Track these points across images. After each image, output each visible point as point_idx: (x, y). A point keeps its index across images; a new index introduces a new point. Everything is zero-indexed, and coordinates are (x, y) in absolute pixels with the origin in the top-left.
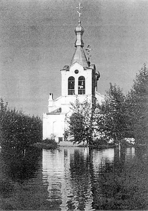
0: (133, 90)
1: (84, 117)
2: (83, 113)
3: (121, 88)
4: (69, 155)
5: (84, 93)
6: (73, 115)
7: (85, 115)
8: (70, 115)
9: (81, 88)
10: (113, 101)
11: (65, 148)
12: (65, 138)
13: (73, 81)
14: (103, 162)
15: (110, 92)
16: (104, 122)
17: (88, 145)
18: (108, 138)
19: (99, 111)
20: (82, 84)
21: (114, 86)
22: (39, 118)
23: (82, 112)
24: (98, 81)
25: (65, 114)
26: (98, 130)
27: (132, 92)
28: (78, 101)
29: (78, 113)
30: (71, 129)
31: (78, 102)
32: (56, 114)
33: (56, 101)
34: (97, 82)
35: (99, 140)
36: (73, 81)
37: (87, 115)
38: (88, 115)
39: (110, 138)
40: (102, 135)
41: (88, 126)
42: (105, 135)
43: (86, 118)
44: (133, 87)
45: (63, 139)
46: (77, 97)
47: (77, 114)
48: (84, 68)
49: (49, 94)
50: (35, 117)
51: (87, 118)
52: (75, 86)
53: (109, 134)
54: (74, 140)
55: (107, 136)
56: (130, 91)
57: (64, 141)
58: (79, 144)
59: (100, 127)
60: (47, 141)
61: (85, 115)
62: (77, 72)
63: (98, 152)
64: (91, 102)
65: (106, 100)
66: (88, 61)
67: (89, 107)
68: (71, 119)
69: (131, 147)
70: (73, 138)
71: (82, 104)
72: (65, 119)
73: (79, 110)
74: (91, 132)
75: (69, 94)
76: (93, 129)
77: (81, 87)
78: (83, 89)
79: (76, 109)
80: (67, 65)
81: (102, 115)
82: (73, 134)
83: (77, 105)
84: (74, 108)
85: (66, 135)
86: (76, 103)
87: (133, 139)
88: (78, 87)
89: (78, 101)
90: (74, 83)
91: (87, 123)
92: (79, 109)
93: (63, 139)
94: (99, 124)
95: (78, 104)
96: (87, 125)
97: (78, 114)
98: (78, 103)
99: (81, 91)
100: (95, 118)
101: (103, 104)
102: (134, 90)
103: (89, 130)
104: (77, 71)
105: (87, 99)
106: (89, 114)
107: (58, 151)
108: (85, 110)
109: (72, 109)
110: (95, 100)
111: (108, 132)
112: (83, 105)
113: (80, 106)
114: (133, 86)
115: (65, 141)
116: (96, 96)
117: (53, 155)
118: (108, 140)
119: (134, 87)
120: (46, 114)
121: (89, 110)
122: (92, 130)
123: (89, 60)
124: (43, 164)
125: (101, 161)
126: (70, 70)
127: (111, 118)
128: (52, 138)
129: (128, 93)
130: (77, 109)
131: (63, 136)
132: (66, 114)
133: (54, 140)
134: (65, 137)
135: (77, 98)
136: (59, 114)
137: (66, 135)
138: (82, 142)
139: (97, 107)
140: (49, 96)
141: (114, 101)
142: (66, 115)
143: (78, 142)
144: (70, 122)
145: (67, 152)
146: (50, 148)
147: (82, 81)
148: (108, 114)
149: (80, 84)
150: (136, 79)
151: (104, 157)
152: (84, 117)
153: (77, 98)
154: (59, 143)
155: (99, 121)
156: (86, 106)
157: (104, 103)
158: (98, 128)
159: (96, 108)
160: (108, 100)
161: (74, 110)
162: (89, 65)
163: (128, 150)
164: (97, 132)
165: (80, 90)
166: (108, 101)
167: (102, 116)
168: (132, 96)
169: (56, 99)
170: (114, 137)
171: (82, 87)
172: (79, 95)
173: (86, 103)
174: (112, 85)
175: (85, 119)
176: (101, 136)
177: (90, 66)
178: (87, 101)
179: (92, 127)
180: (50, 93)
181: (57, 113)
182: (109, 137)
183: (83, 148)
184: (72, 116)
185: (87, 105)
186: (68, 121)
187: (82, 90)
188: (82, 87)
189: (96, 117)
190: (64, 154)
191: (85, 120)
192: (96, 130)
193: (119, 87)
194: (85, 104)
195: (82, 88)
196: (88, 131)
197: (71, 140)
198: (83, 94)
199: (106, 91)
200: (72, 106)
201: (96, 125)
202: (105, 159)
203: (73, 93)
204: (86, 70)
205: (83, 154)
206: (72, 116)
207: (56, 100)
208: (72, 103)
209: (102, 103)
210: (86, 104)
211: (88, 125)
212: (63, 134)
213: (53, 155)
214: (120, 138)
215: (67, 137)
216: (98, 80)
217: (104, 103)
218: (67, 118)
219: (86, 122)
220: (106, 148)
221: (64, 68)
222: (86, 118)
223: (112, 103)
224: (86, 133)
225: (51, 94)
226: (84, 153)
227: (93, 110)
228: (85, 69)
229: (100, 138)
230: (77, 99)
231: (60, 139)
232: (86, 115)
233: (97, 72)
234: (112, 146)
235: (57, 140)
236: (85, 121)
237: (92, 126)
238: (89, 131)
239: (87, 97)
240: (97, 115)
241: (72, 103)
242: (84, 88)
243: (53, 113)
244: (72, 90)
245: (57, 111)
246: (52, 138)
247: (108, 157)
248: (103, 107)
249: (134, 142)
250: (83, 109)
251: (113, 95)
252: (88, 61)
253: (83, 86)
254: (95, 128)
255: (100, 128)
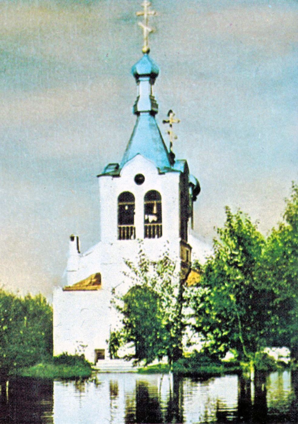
0: (284, 225)
1: (160, 295)
2: (156, 285)
3: (252, 221)
4: (121, 394)
5: (160, 233)
6: (133, 290)
7: (163, 290)
8: (124, 290)
9: (150, 221)
10: (233, 252)
11: (113, 378)
12: (110, 352)
13: (129, 203)
14: (211, 409)
15: (226, 231)
16: (213, 308)
17: (172, 368)
18: (222, 348)
19: (198, 281)
20: (155, 211)
21: (235, 216)
22: (45, 301)
23: (154, 284)
24: (194, 203)
25: (111, 289)
26: (198, 330)
27: (283, 231)
28: (143, 255)
29: (143, 286)
30: (128, 326)
31: (143, 257)
32: (88, 290)
33: (87, 257)
34: (192, 204)
35: (201, 355)
36: (129, 203)
37: (168, 290)
38: (171, 291)
39: (227, 350)
40: (208, 340)
41: (171, 320)
42: (213, 342)
43: (165, 299)
44: (284, 217)
45: (107, 354)
46: (141, 244)
47: (142, 287)
48: (158, 169)
49: (69, 240)
50: (33, 297)
51: (168, 299)
52: (136, 217)
53: (224, 339)
54: (135, 357)
55: (219, 343)
56: (277, 229)
57: (109, 359)
58: (149, 365)
59: (201, 321)
60: (65, 359)
61: (163, 290)
62: (139, 179)
63: (196, 390)
64: (177, 257)
65: (216, 252)
66: (169, 152)
67: (172, 269)
68: (126, 301)
69: (281, 372)
70: (132, 351)
71: (155, 264)
72: (111, 302)
73: (145, 278)
74: (179, 333)
75: (120, 238)
76: (183, 326)
77: (152, 218)
78: (156, 224)
79: (138, 275)
80: (115, 162)
81: (206, 289)
82: (132, 340)
83: (141, 266)
84: (133, 275)
85: (114, 342)
86: (139, 260)
87: (285, 352)
88: (143, 218)
89: (143, 255)
90: (132, 207)
91: (167, 311)
92: (147, 275)
93: (107, 354)
94: (200, 313)
95: (143, 262)
96: (169, 315)
97: (146, 289)
98: (143, 260)
99: (152, 230)
100: (189, 297)
101: (209, 263)
102: (287, 225)
103: (173, 329)
104: (141, 178)
105: (167, 250)
106: (172, 287)
107: (92, 385)
108: (162, 278)
109: (128, 276)
110: (187, 252)
111: (222, 332)
112: (156, 266)
113: (151, 268)
114: (283, 214)
115: (111, 358)
116: (191, 240)
117: (80, 396)
118: (223, 354)
119: (286, 217)
120: (61, 289)
121: (173, 276)
122: (181, 329)
123: (171, 149)
124: (54, 419)
125: (206, 408)
126: (121, 174)
127: (228, 298)
128: (76, 351)
129: (271, 233)
130: (141, 275)
131: (106, 347)
132: (114, 289)
133: (83, 355)
134: (112, 348)
135: (141, 248)
136: (96, 290)
137: (113, 343)
138: (156, 362)
139: (195, 271)
140: (68, 243)
141: (237, 253)
142: (113, 293)
143: (143, 362)
144: (123, 310)
145: (116, 388)
146: (74, 378)
147: (155, 202)
148: (223, 288)
149: (148, 209)
150: (292, 196)
151: (213, 399)
152: (160, 297)
153: (140, 246)
154: (95, 364)
155: (198, 305)
156: (164, 269)
157: (212, 258)
158: (198, 322)
159: (192, 272)
160: (221, 251)
161: (134, 279)
162: (172, 162)
163: (273, 377)
164: (194, 334)
165: (150, 227)
166: (222, 253)
167: (207, 293)
168: (282, 241)
169: (87, 250)
170: (236, 345)
171: (154, 218)
172: (147, 239)
173: (165, 261)
174: (231, 211)
175: (163, 300)
176: (205, 344)
177: (175, 165)
178: (168, 255)
179: (180, 321)
180: (70, 234)
181: (92, 287)
182: (225, 346)
183: (159, 376)
184: (130, 294)
185: (167, 265)
186: (118, 308)
187: (154, 227)
188: (154, 218)
189: (190, 295)
190: (108, 392)
191: (164, 304)
192: (191, 330)
193: (248, 216)
194: (161, 262)
195: (153, 222)
196: (170, 332)
197: (126, 356)
198: (156, 236)
199: (216, 228)
200: (128, 268)
201: (192, 316)
202: (216, 402)
203: (132, 233)
204: (163, 173)
205: (158, 391)
206: (130, 294)
207: (87, 252)
208: (128, 259)
209: (206, 258)
210: (165, 262)
211: (170, 316)
212: (107, 341)
213: (80, 396)
214: (253, 348)
215: (116, 347)
216: (194, 199)
217: (210, 259)
218: (115, 300)
219: (164, 308)
220: (218, 375)
221: (108, 171)
222: (165, 299)
223: (232, 258)
224: (165, 338)
225: (72, 239)
226: (160, 389)
227: (184, 278)
228: (161, 172)
229: (201, 351)
230: (141, 251)
231: (100, 355)
232: (165, 290)
233: (192, 180)
234: (232, 369)
235: (90, 358)
236: (162, 307)
237: (181, 318)
238: (172, 333)
239: (166, 244)
240: (194, 291)
241: (129, 261)
242: (160, 220)
243: (79, 287)
244: (128, 228)
245: (89, 282)
246: (78, 351)
247: (222, 398)
248: (209, 269)
249: (287, 357)
250: (157, 275)
251: (235, 238)
252: (169, 152)
253: (155, 214)
254: (190, 325)
255: (202, 323)
